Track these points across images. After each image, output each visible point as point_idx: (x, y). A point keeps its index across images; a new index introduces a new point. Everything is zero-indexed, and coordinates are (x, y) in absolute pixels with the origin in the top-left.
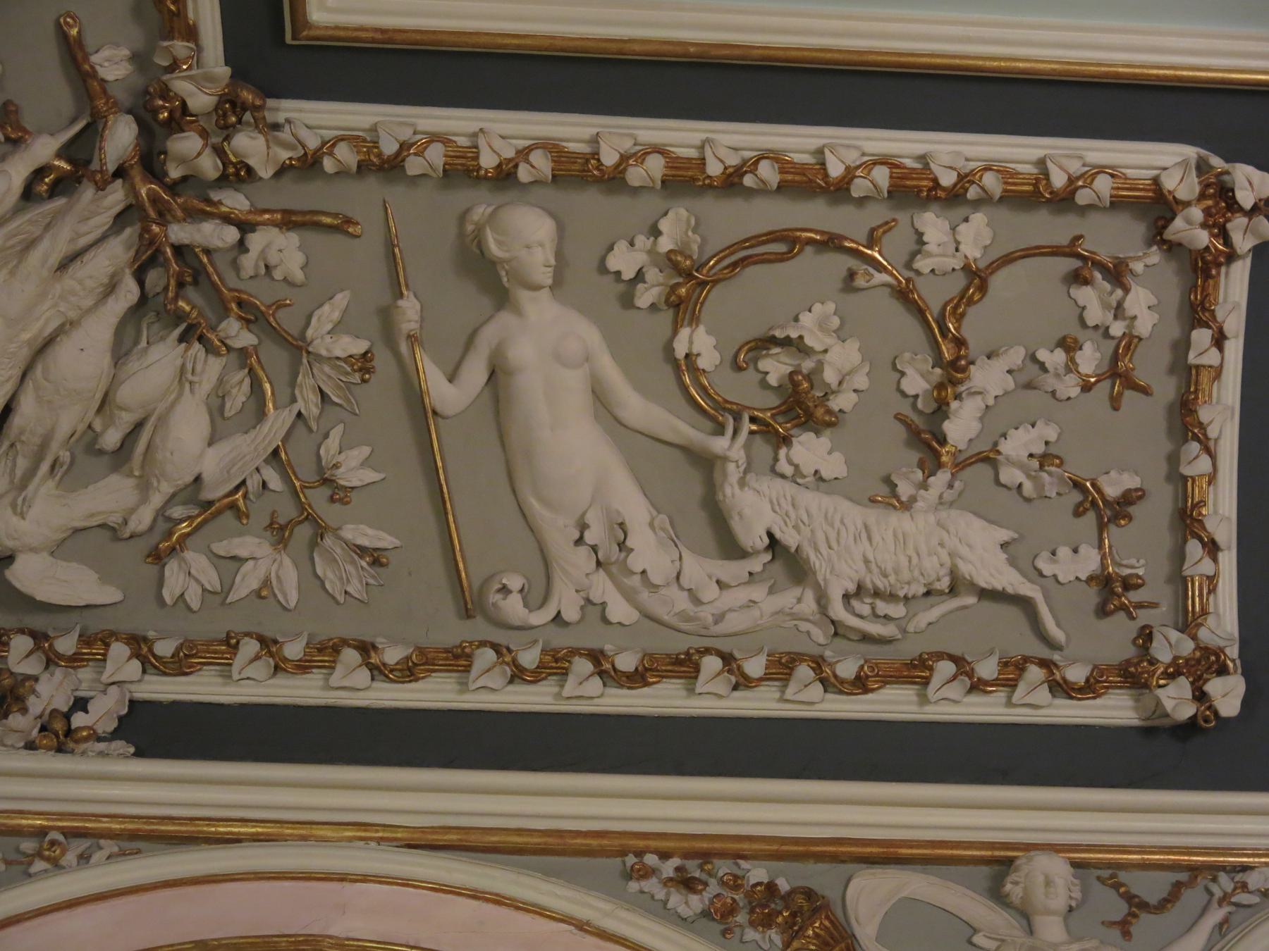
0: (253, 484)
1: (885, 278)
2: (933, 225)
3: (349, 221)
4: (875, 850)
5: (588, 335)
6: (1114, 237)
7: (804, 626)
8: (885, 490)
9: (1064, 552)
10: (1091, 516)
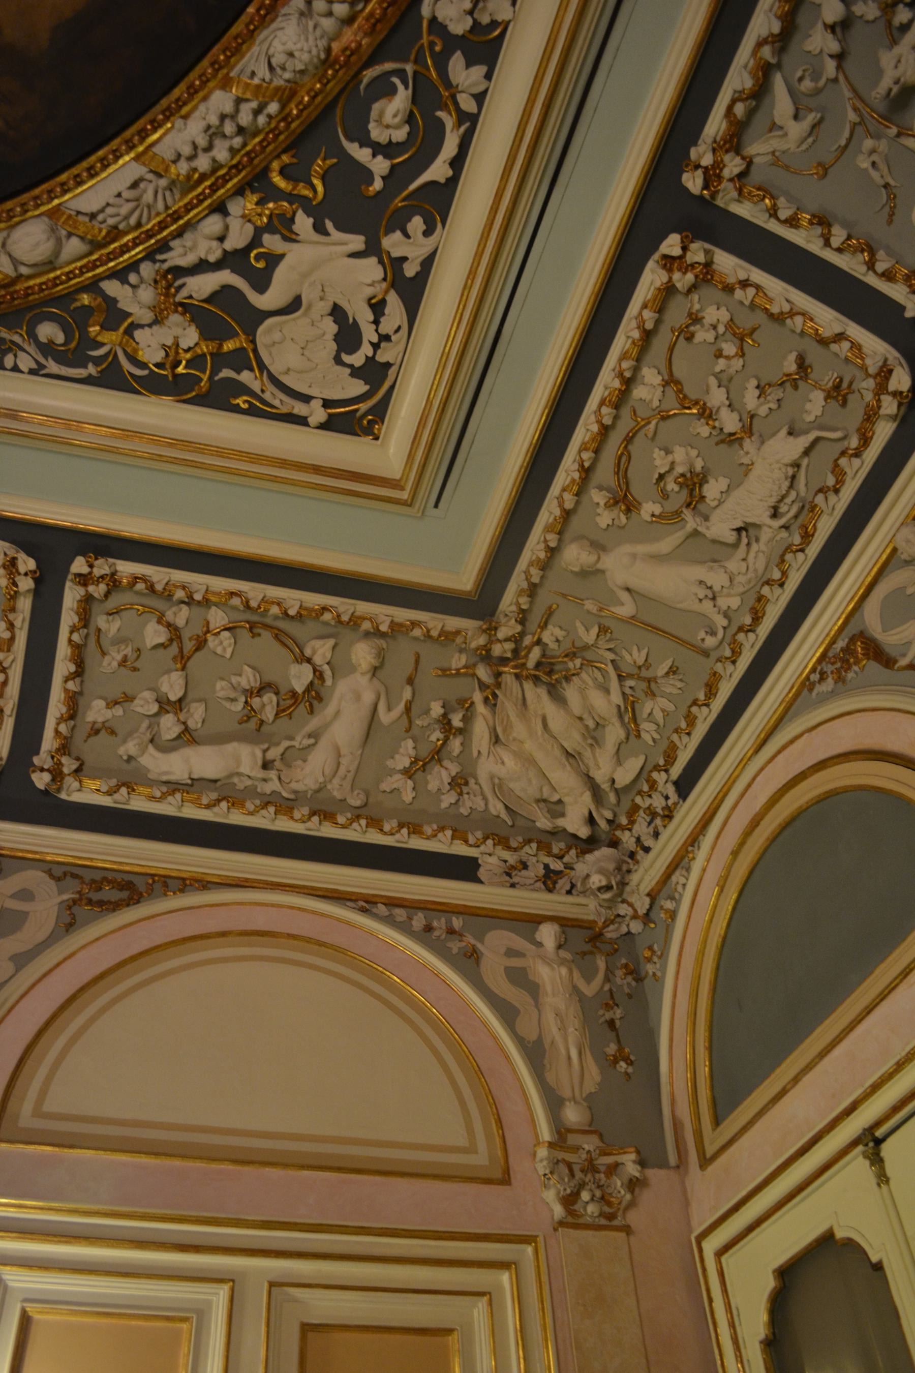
0: (628, 691)
1: (654, 422)
2: (639, 392)
3: (550, 607)
4: (862, 591)
5: (627, 548)
6: (676, 315)
7: (778, 538)
8: (744, 468)
9: (808, 406)
10: (800, 383)
